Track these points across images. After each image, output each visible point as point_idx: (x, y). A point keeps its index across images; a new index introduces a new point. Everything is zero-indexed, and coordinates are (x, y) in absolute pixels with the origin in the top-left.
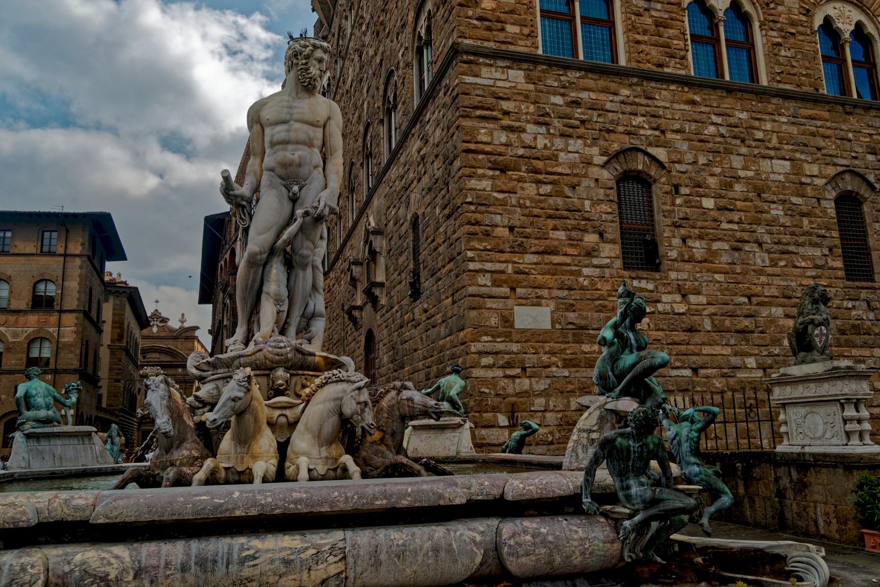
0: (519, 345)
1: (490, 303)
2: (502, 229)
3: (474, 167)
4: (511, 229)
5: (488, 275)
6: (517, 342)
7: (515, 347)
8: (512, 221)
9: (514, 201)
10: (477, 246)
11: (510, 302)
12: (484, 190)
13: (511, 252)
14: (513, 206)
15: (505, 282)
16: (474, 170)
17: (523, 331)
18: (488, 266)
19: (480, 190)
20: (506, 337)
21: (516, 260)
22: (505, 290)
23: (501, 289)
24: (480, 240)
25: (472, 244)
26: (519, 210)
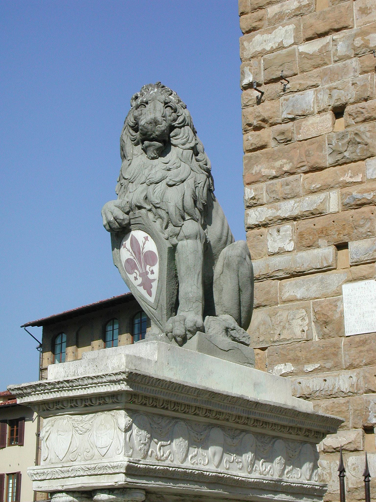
0: (353, 373)
1: (292, 289)
2: (316, 119)
3: (260, 8)
4: (338, 112)
5: (287, 227)
6: (351, 367)
7: (344, 381)
8: (336, 94)
9: (342, 49)
10: (266, 171)
11: (332, 278)
12: (281, 47)
13: (337, 164)
14: (341, 59)
15: (323, 232)
16: (260, 13)
17: (363, 340)
18: (288, 208)
19: (272, 51)
20: (325, 357)
21: (347, 178)
22: (325, 252)
23: (315, 251)
24: (272, 157)
25: (256, 169)
26: (354, 63)
